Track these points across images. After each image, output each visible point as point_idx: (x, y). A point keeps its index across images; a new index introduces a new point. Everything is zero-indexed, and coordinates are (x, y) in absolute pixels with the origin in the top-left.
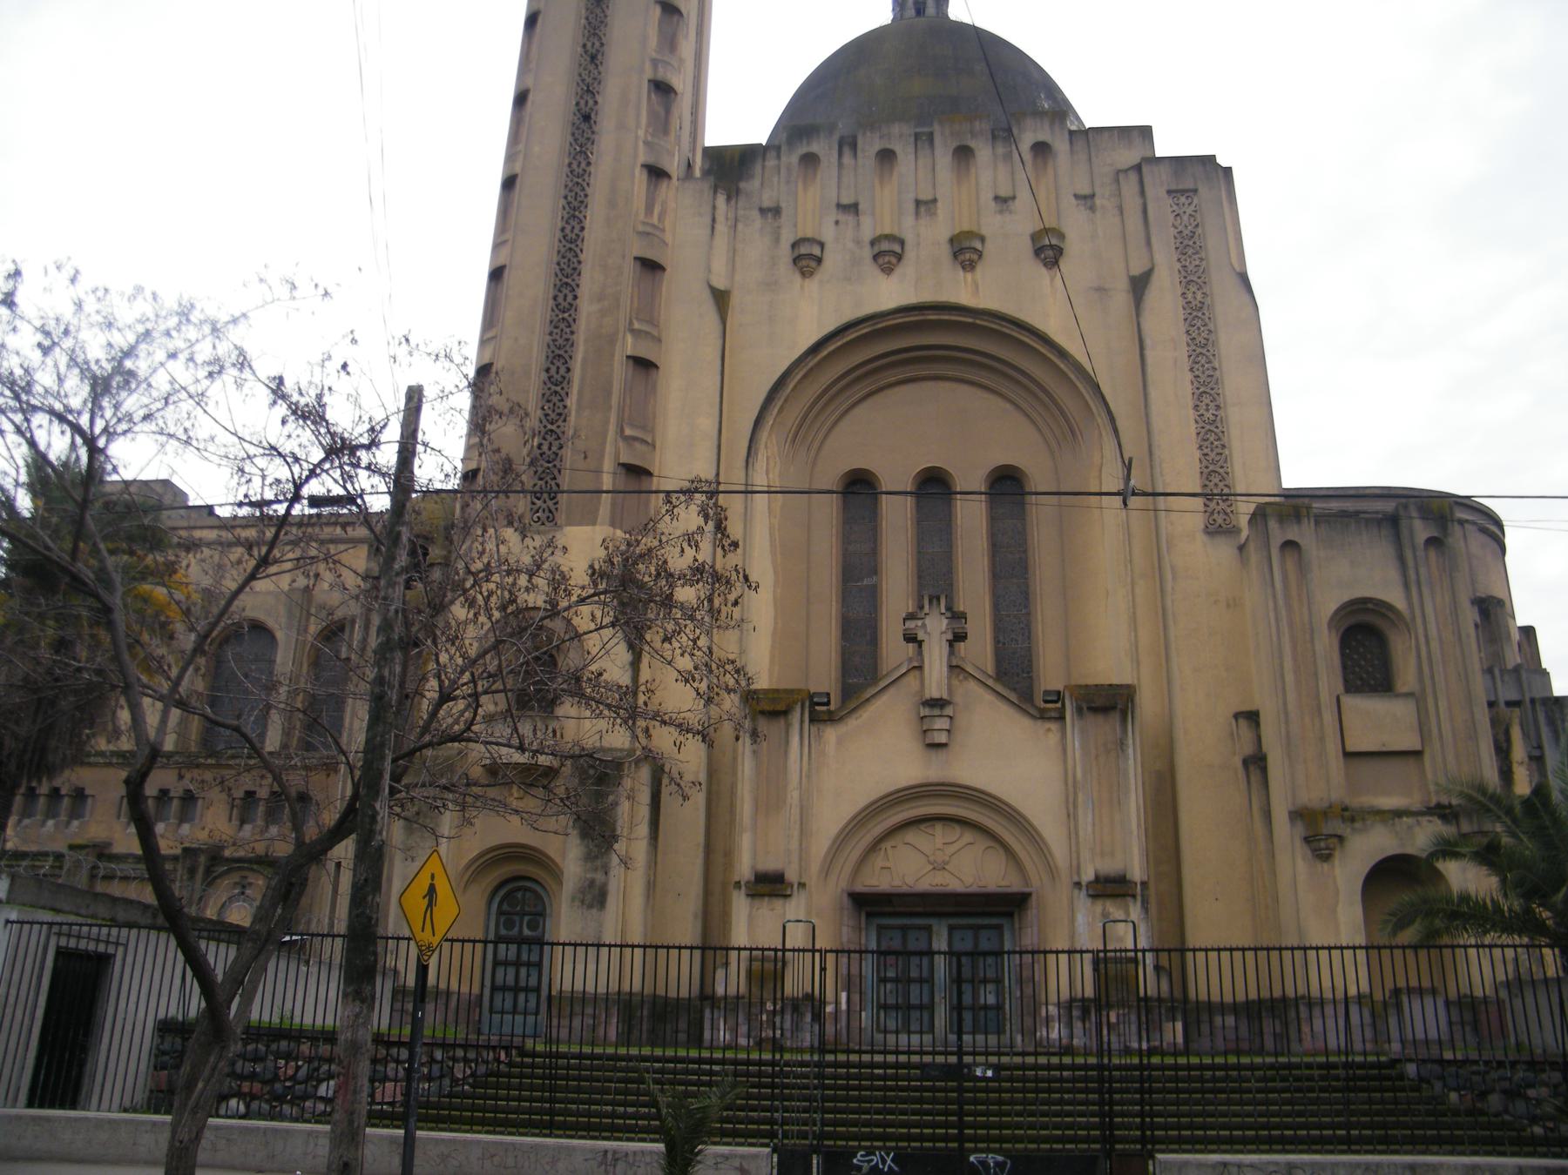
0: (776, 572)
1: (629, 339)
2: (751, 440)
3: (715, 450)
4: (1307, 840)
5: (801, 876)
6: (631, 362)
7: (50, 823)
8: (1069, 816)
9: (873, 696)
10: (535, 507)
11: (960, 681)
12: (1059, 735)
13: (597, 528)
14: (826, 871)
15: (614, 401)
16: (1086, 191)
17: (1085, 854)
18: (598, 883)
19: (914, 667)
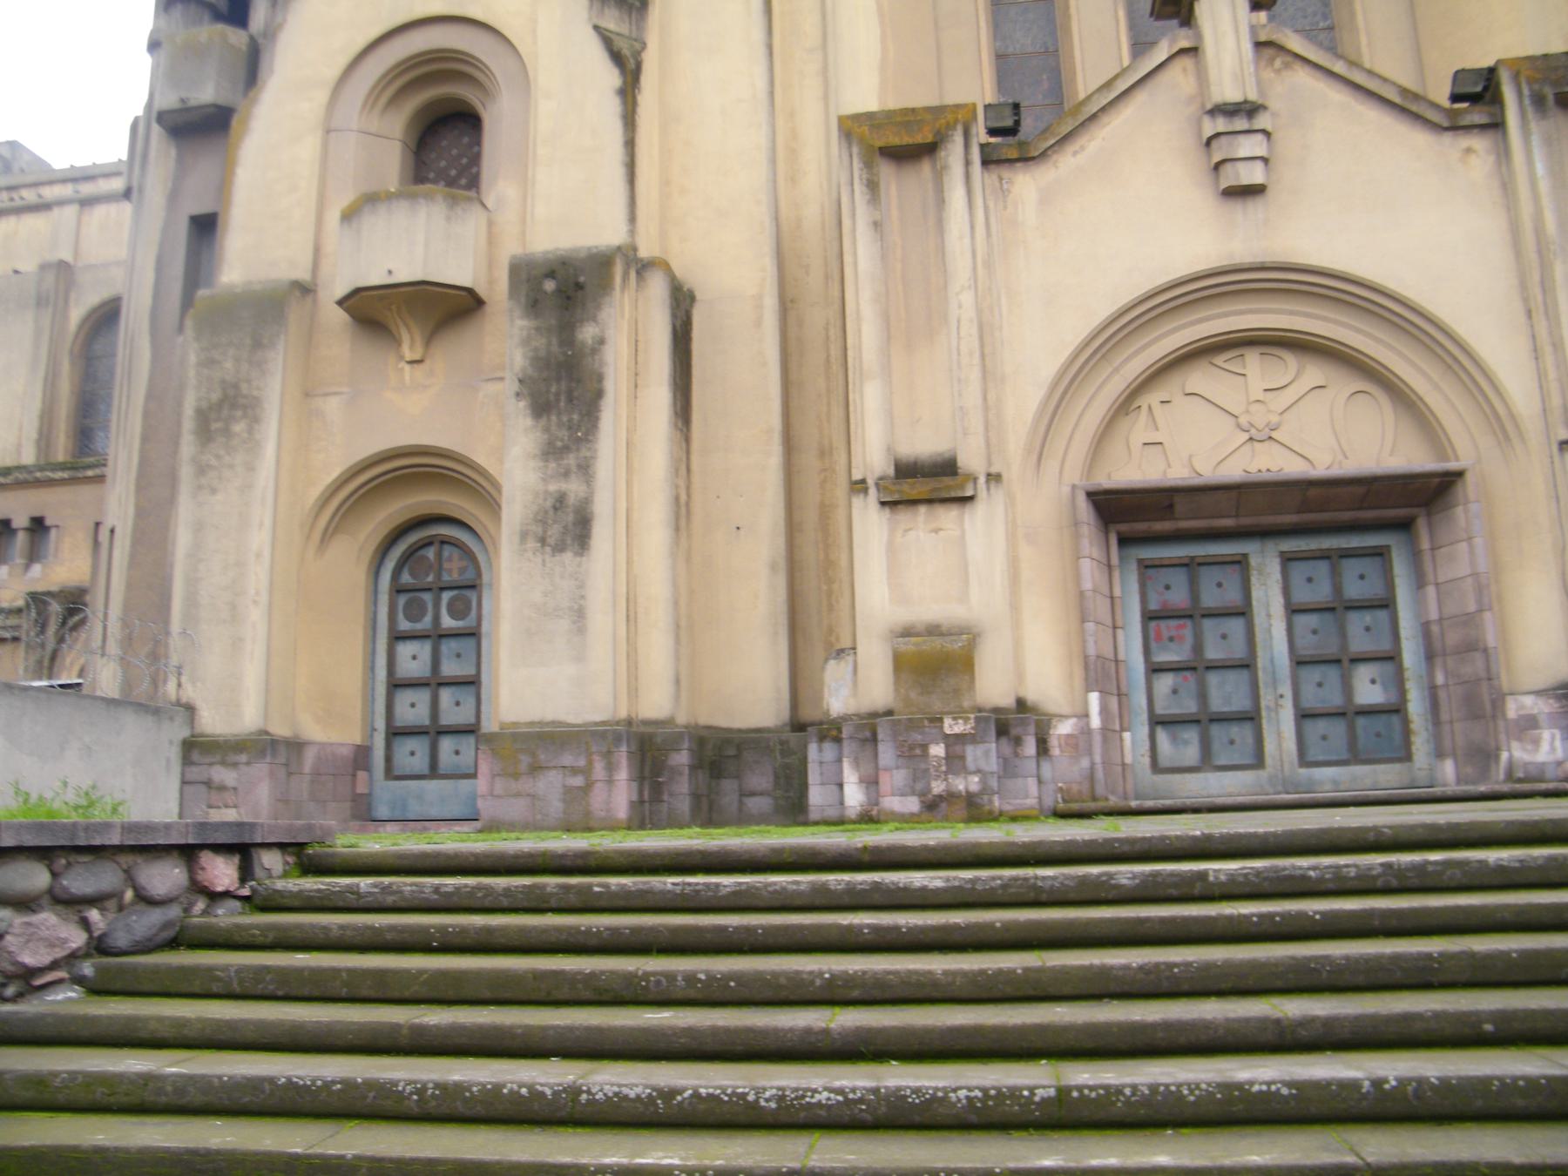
5: (990, 464)
8: (1529, 314)
9: (1103, 109)
11: (1278, 71)
14: (1039, 452)
18: (572, 500)
19: (1182, 51)
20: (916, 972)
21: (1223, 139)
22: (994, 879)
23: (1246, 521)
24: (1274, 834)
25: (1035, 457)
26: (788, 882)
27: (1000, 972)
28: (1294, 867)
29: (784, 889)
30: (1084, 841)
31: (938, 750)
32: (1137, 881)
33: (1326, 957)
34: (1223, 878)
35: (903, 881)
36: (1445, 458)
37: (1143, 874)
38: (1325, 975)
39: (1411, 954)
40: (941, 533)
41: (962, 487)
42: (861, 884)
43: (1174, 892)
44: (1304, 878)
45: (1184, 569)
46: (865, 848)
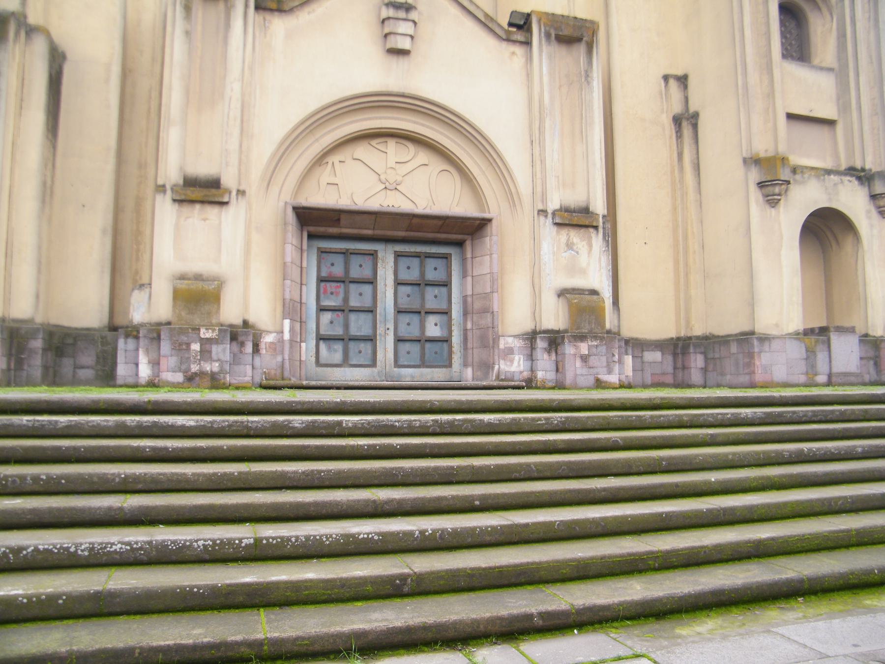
4: (761, 185)
5: (239, 184)
12: (523, 60)
14: (269, 181)
17: (551, 183)
20: (176, 474)
21: (391, 21)
22: (224, 421)
23: (379, 232)
24: (379, 403)
25: (266, 184)
26: (101, 421)
27: (225, 474)
28: (388, 420)
29: (99, 425)
30: (276, 402)
31: (196, 347)
32: (304, 425)
33: (401, 468)
34: (350, 425)
35: (171, 421)
36: (484, 211)
37: (307, 421)
38: (400, 477)
39: (444, 467)
40: (207, 221)
41: (222, 196)
42: (146, 422)
43: (324, 432)
44: (393, 426)
45: (342, 256)
46: (149, 401)
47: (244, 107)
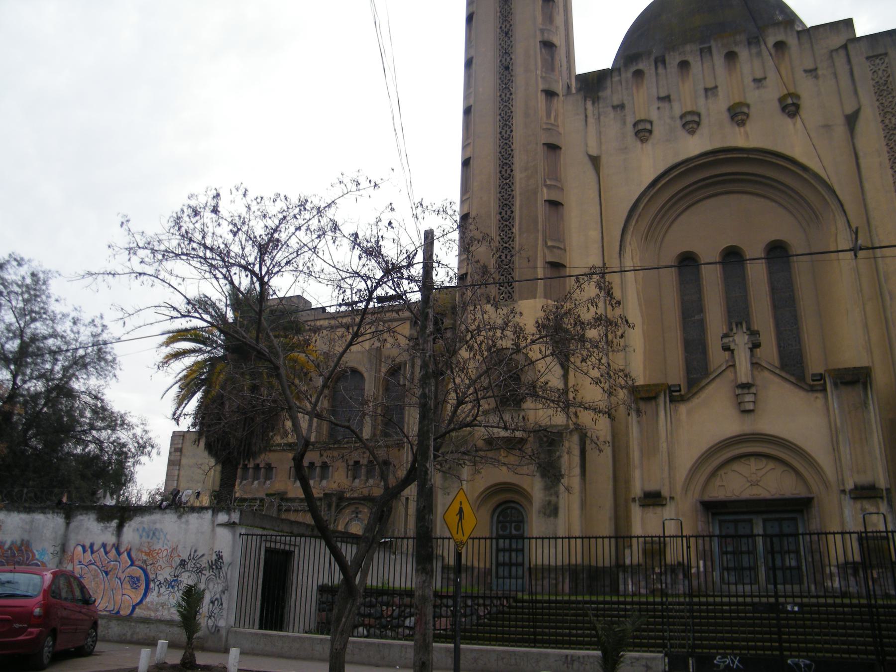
0: (642, 316)
1: (545, 190)
2: (621, 241)
3: (601, 249)
5: (671, 494)
6: (547, 204)
7: (256, 482)
8: (834, 449)
9: (707, 384)
10: (501, 292)
13: (537, 300)
15: (540, 227)
16: (811, 66)
47: (670, 454)
